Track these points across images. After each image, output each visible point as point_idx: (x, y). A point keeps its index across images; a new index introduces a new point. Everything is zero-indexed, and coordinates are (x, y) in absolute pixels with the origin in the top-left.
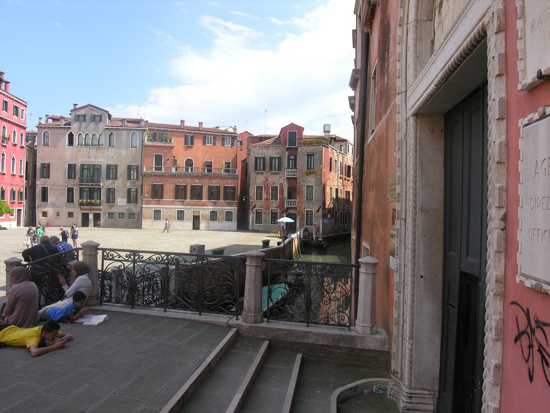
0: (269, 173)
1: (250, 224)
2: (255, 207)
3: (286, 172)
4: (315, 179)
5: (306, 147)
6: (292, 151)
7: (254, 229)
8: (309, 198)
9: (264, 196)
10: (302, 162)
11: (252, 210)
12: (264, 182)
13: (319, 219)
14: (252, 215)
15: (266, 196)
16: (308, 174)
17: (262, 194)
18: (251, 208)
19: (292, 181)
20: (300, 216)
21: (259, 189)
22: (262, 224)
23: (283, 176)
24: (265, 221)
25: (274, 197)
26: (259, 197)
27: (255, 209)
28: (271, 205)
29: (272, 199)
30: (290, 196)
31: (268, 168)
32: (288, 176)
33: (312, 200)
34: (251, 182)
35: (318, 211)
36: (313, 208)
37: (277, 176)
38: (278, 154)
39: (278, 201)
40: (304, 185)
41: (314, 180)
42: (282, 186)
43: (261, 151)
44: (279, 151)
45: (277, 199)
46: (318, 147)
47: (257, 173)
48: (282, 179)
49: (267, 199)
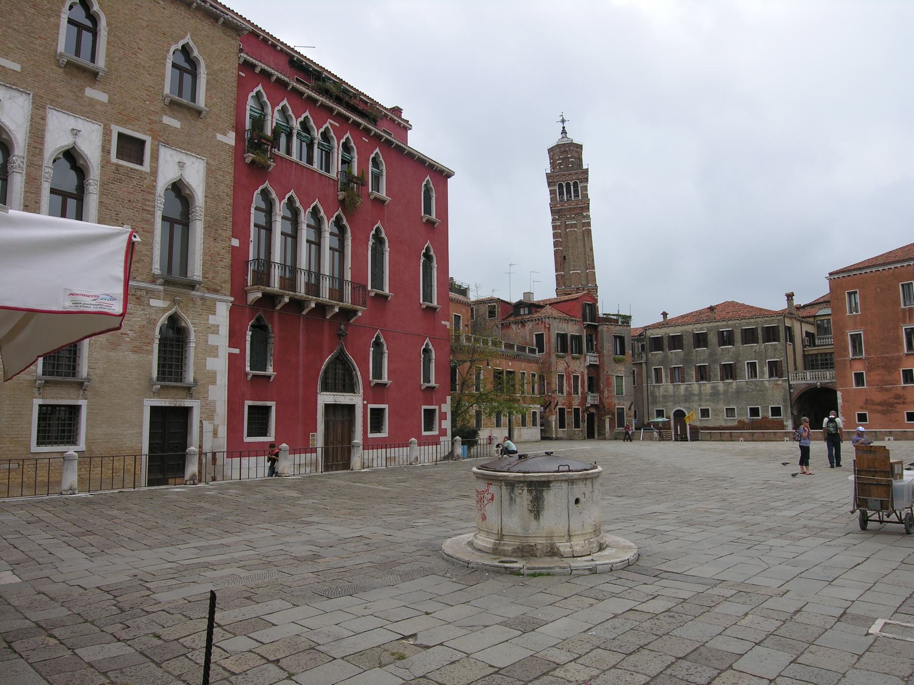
0: (570, 357)
1: (554, 429)
2: (557, 405)
3: (588, 357)
4: (625, 368)
5: (613, 326)
6: (593, 330)
7: (558, 437)
8: (620, 393)
9: (565, 388)
10: (608, 346)
11: (555, 409)
12: (566, 369)
13: (631, 418)
14: (555, 416)
15: (568, 389)
16: (617, 361)
17: (563, 385)
18: (553, 405)
19: (591, 369)
20: (610, 416)
21: (561, 377)
22: (566, 429)
23: (583, 362)
24: (568, 425)
25: (576, 392)
26: (561, 391)
27: (558, 407)
28: (573, 402)
29: (574, 394)
30: (591, 389)
31: (569, 349)
32: (591, 363)
33: (622, 393)
34: (553, 369)
35: (630, 409)
36: (624, 405)
37: (578, 361)
38: (577, 332)
39: (580, 394)
40: (613, 375)
41: (623, 369)
42: (583, 376)
43: (560, 325)
44: (577, 327)
45: (578, 394)
46: (625, 328)
47: (558, 357)
48: (582, 366)
49: (569, 394)
